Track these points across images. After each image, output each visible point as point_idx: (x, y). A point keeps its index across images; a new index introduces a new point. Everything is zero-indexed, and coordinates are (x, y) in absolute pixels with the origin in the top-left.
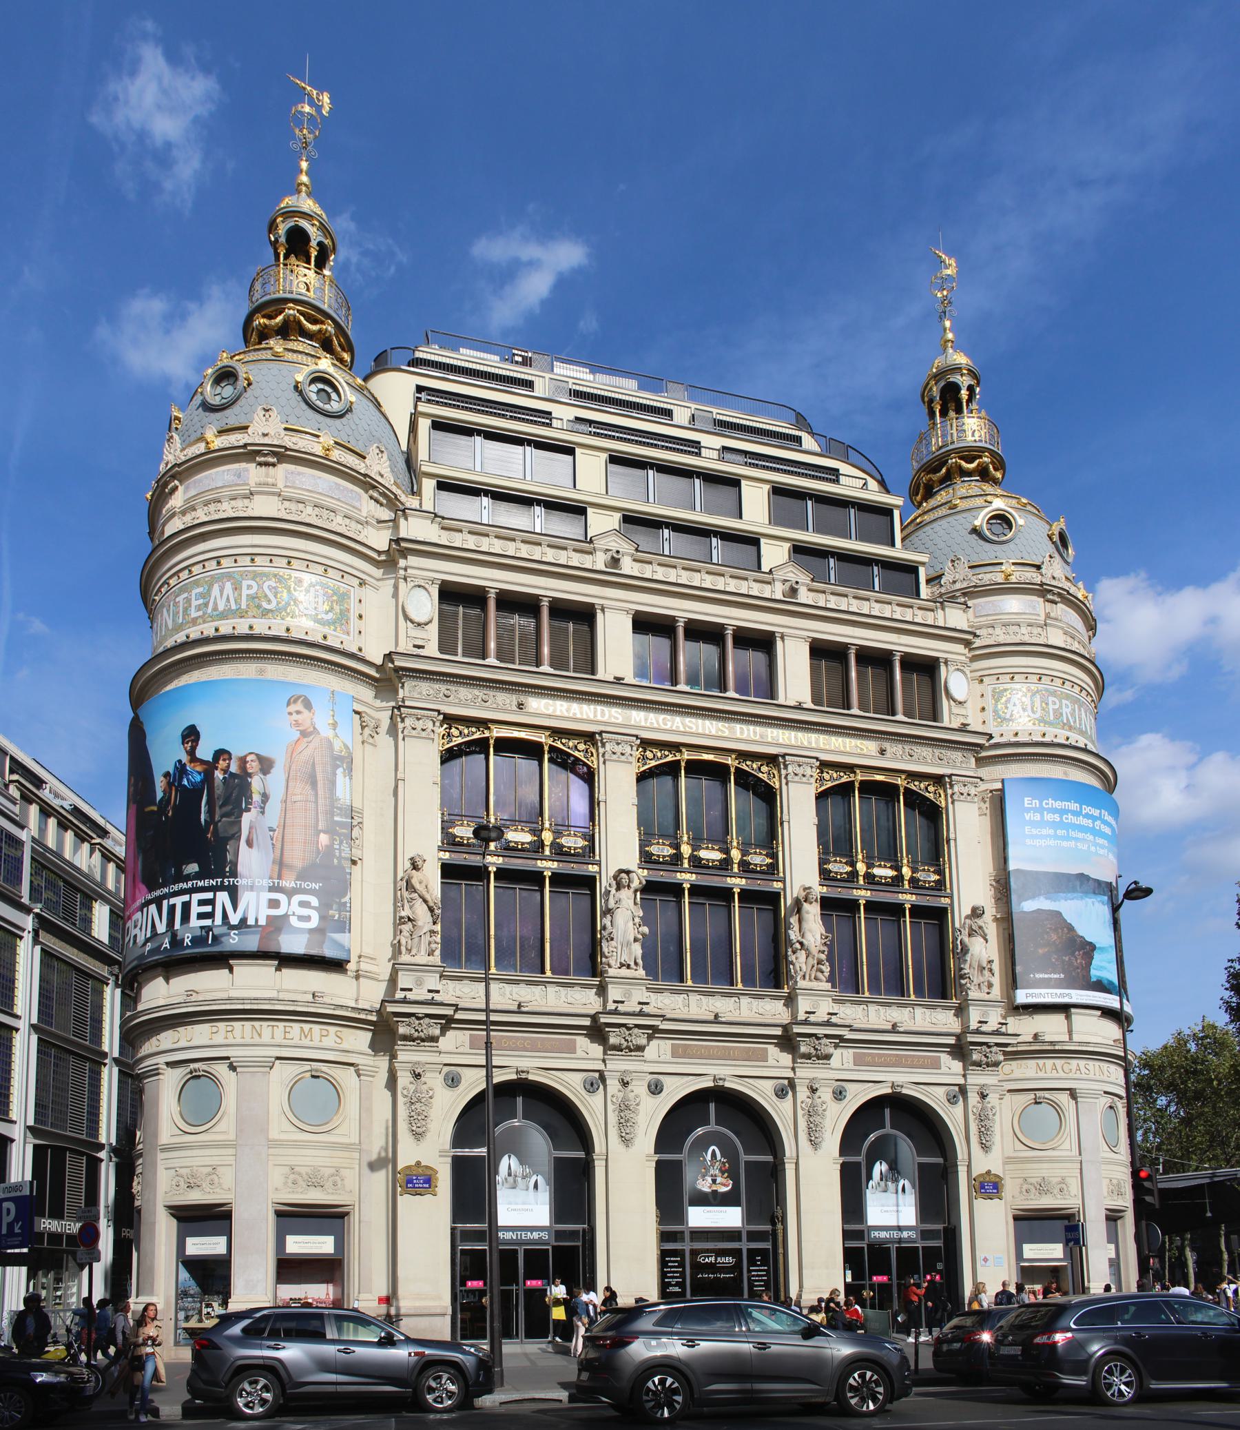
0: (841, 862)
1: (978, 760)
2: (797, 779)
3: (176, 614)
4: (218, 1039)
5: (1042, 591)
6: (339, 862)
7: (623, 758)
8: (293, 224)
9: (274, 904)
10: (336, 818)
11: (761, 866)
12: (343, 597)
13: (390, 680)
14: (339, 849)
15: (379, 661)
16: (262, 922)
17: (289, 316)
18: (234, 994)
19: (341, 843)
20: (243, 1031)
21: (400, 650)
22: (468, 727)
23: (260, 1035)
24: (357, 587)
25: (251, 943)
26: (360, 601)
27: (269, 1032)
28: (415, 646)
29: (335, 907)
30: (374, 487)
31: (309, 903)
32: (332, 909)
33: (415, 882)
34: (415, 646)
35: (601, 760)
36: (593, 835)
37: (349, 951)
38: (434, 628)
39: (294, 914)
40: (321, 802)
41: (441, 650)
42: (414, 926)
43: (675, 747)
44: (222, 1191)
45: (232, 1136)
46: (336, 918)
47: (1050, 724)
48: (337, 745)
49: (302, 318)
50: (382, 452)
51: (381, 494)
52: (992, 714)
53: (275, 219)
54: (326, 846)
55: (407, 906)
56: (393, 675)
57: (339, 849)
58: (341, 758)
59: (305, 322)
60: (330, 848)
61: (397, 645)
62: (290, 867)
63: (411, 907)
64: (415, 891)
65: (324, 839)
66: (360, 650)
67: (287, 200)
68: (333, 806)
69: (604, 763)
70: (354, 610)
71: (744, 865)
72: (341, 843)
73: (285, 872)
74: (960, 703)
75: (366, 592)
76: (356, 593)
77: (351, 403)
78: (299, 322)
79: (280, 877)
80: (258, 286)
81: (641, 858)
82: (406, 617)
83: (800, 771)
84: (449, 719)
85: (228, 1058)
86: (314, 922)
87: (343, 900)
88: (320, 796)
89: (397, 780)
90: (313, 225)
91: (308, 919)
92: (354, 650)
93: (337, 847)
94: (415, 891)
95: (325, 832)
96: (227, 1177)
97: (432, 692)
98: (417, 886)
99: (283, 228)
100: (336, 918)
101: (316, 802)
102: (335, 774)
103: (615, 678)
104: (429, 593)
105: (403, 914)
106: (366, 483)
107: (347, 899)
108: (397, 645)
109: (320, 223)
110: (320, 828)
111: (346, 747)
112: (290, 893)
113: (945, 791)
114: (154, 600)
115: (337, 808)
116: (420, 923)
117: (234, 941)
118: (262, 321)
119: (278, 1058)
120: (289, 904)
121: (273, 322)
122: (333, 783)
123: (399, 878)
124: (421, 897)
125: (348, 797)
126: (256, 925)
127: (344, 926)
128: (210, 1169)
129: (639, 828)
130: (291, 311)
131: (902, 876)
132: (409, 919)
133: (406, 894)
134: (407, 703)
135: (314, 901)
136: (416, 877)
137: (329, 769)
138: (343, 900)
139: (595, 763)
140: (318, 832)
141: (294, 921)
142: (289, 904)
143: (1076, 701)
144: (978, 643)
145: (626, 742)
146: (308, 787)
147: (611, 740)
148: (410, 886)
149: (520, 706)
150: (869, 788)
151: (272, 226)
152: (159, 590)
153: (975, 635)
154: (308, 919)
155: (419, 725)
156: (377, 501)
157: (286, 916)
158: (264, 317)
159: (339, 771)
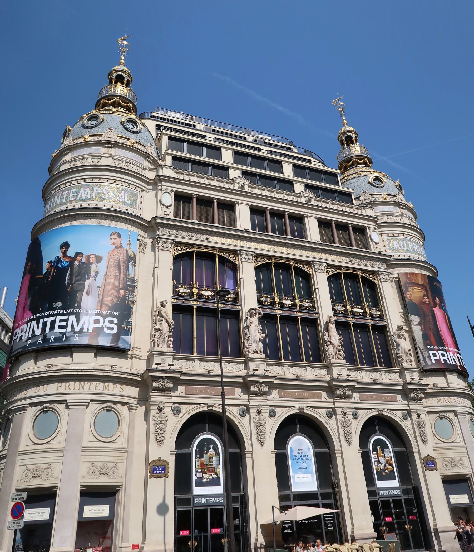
0: (340, 306)
1: (387, 265)
2: (319, 271)
3: (62, 199)
4: (61, 390)
5: (398, 205)
6: (128, 303)
7: (249, 261)
8: (119, 74)
9: (97, 322)
10: (128, 283)
11: (308, 307)
12: (136, 195)
13: (152, 227)
14: (129, 297)
15: (149, 219)
16: (91, 330)
17: (116, 100)
18: (73, 366)
19: (129, 295)
20: (74, 386)
21: (158, 215)
22: (185, 247)
23: (83, 388)
24: (140, 191)
25: (85, 341)
26: (141, 197)
27: (88, 387)
28: (165, 214)
29: (125, 323)
30: (149, 157)
31: (113, 321)
32: (123, 325)
33: (163, 312)
34: (165, 214)
35: (240, 262)
36: (238, 292)
37: (130, 345)
38: (172, 208)
39: (106, 327)
40: (122, 276)
41: (174, 216)
42: (161, 333)
43: (270, 257)
44: (53, 479)
45: (62, 445)
46: (125, 329)
47: (411, 253)
48: (130, 253)
49: (121, 101)
50: (152, 145)
51: (151, 159)
52: (388, 248)
53: (112, 72)
54: (123, 295)
55: (158, 324)
56: (155, 225)
57: (129, 297)
58: (131, 258)
59: (122, 102)
60: (124, 296)
61: (157, 213)
62: (106, 305)
63: (160, 324)
64: (163, 317)
65: (122, 292)
66: (141, 215)
67: (117, 67)
68: (127, 278)
69: (242, 263)
70: (139, 200)
71: (301, 306)
72: (129, 295)
73: (103, 307)
74: (377, 243)
75: (144, 194)
76: (140, 194)
77: (141, 129)
78: (119, 102)
79: (100, 309)
80: (104, 91)
81: (258, 303)
82: (161, 203)
83: (320, 268)
84: (177, 244)
85: (65, 401)
86: (115, 331)
87: (129, 320)
88: (121, 273)
89: (155, 268)
90: (126, 74)
91: (112, 329)
92: (138, 215)
93: (128, 296)
94: (163, 317)
95: (122, 289)
96: (57, 470)
97: (171, 232)
98: (164, 314)
99: (114, 75)
100: (125, 329)
101: (120, 276)
102: (128, 265)
103: (245, 229)
104: (171, 195)
105: (157, 327)
106: (146, 156)
107: (131, 319)
108: (157, 213)
109: (129, 74)
110: (121, 287)
111: (134, 254)
112: (105, 317)
113: (377, 277)
114: (51, 193)
115: (129, 279)
116: (164, 332)
117: (76, 340)
118: (105, 101)
119: (92, 401)
120: (104, 322)
121: (109, 102)
122: (127, 268)
123: (154, 311)
124: (165, 319)
125: (133, 274)
126: (88, 332)
127: (128, 332)
128: (47, 465)
129: (257, 290)
130: (117, 99)
131: (347, 310)
132: (159, 330)
133: (158, 318)
134: (160, 236)
135: (116, 321)
136: (163, 310)
137: (126, 263)
138: (129, 320)
139: (237, 262)
140: (119, 291)
141: (106, 330)
142: (104, 322)
143: (418, 244)
144: (379, 221)
145: (250, 254)
146: (116, 269)
147: (244, 253)
148: (160, 314)
149: (207, 239)
150: (347, 276)
151: (111, 73)
152: (55, 189)
153: (379, 219)
154: (112, 329)
155: (165, 245)
156: (149, 162)
157: (102, 327)
158: (105, 100)
159: (131, 263)
